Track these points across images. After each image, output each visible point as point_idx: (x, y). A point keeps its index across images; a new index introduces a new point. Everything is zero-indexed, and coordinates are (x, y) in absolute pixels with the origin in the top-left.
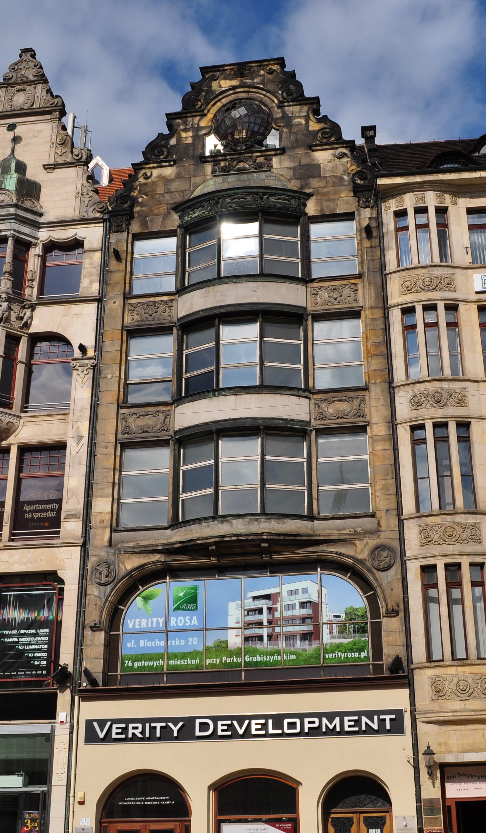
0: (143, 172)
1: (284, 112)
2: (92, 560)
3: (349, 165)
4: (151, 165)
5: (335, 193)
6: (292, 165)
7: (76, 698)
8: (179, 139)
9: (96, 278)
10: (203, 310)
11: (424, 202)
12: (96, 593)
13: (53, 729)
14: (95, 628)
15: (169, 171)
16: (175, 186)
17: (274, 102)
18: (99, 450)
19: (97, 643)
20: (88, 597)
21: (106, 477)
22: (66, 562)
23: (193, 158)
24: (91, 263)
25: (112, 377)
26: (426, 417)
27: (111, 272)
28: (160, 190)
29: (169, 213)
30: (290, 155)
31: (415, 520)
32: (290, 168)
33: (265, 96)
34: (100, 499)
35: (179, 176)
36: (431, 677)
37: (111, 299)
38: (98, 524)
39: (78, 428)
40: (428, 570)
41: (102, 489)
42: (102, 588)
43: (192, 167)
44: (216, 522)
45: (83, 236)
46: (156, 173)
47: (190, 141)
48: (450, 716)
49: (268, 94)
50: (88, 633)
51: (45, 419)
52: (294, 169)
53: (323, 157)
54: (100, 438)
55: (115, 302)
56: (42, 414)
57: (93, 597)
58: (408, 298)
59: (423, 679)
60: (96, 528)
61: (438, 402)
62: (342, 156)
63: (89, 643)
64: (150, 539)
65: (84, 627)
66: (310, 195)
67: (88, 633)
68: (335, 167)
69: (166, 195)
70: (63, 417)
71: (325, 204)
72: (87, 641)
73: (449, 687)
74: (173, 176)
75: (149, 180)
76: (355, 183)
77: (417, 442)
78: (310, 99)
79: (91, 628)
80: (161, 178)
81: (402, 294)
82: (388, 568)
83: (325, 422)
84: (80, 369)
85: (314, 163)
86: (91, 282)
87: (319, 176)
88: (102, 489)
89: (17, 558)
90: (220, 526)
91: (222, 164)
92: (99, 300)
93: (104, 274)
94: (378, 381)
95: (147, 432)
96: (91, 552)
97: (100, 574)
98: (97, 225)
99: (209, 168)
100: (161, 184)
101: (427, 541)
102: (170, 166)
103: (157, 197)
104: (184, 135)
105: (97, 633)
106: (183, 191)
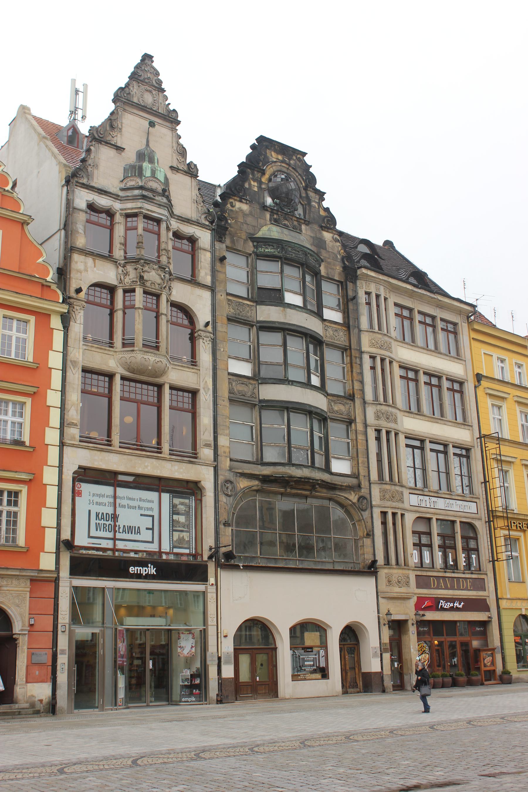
0: (231, 200)
1: (307, 194)
2: (221, 479)
3: (340, 249)
4: (235, 198)
5: (334, 265)
6: (312, 235)
7: (219, 569)
8: (250, 184)
9: (209, 272)
10: (278, 322)
11: (379, 292)
12: (225, 500)
13: (206, 588)
14: (226, 524)
15: (245, 207)
16: (250, 220)
17: (302, 184)
18: (220, 402)
19: (227, 534)
20: (220, 503)
21: (225, 422)
22: (206, 477)
23: (259, 204)
24: (205, 259)
25: (223, 351)
26: (384, 426)
27: (218, 271)
28: (241, 220)
29: (247, 240)
30: (311, 228)
31: (378, 485)
32: (311, 237)
33: (297, 177)
34: (222, 436)
35: (251, 214)
36: (386, 574)
37: (219, 292)
38: (223, 454)
39: (206, 382)
40: (384, 514)
41: (223, 429)
42: (228, 498)
43: (258, 210)
44: (294, 468)
45: (199, 235)
46: (238, 205)
47: (256, 189)
48: (395, 595)
49: (299, 177)
50: (222, 526)
51: (185, 369)
52: (313, 238)
53: (327, 236)
54: (219, 393)
55: (221, 296)
56: (183, 365)
57: (223, 503)
58: (373, 350)
59: (383, 573)
60: (221, 456)
61: (388, 418)
62: (336, 241)
63: (223, 534)
64: (249, 469)
65: (220, 523)
66: (322, 261)
67: (222, 526)
68: (333, 246)
69: (244, 224)
70: (196, 371)
71: (330, 270)
72: (221, 532)
73: (394, 579)
74: (247, 212)
75: (234, 209)
76: (344, 263)
77: (378, 439)
78: (319, 191)
79: (224, 524)
80: (241, 210)
81: (370, 346)
82: (364, 510)
83: (336, 415)
84: (205, 338)
85: (323, 239)
86: (206, 274)
87: (326, 249)
88: (223, 429)
89: (176, 468)
90: (297, 470)
91: (275, 216)
92: (212, 289)
93: (214, 272)
94: (359, 397)
95: (244, 396)
96: (220, 472)
97: (227, 488)
98: (207, 231)
99: (268, 215)
100: (241, 214)
101: (383, 498)
102: (246, 203)
103: (239, 224)
104: (252, 183)
105: (227, 528)
106: (254, 226)
